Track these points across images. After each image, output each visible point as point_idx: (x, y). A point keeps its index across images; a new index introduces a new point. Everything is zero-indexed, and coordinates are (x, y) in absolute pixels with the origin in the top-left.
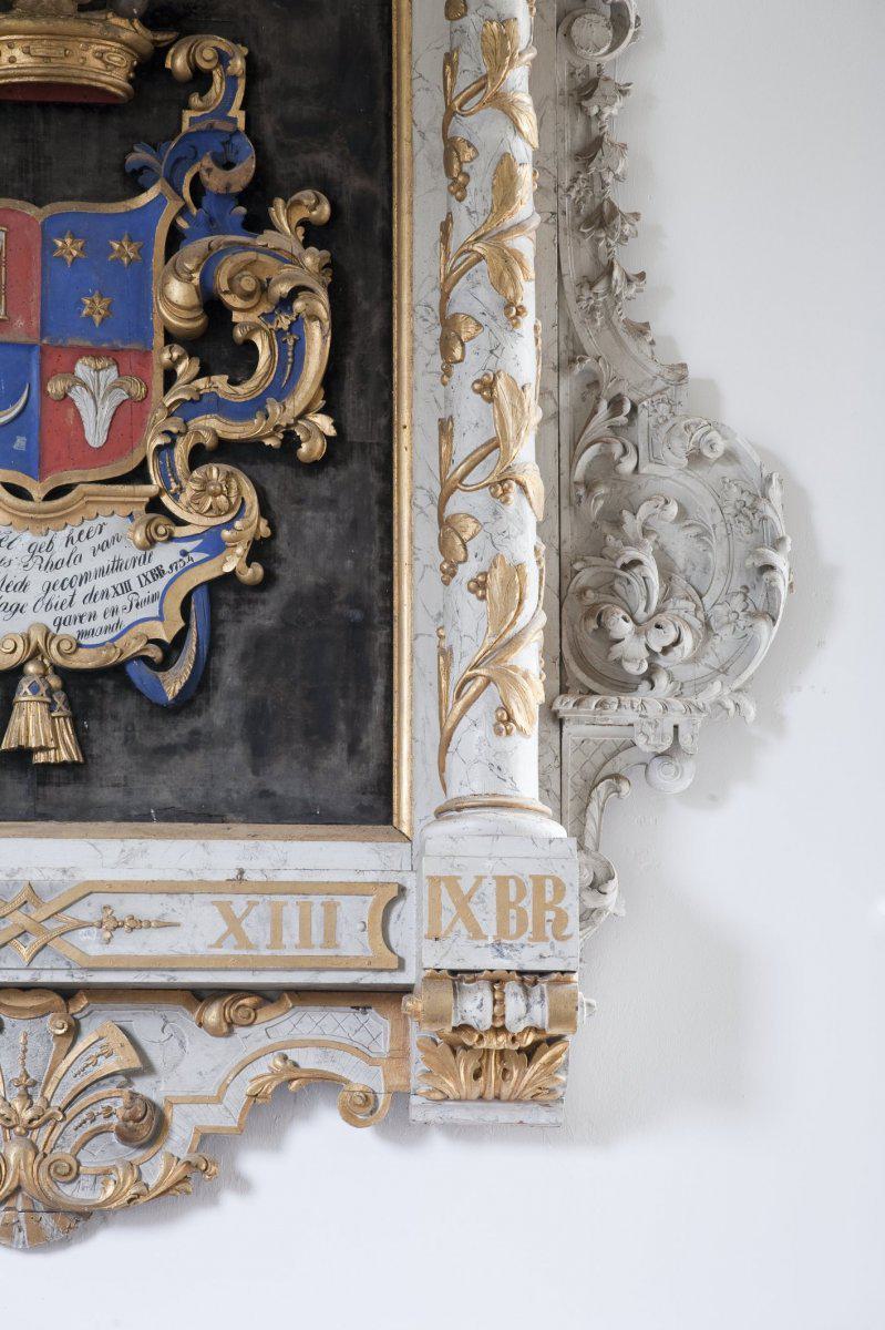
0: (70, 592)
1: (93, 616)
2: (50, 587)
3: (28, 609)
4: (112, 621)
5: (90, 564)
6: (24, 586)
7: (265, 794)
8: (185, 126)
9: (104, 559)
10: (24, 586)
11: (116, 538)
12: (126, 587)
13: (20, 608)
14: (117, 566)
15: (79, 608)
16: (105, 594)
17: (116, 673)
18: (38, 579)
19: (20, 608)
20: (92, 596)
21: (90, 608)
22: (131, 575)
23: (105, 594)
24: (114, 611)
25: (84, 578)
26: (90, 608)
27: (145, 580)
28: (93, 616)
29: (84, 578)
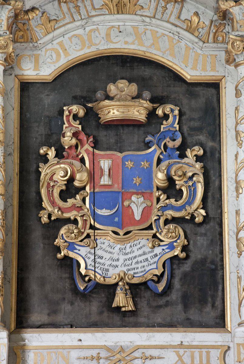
0: (131, 261)
1: (138, 268)
2: (125, 260)
4: (143, 269)
5: (137, 253)
6: (118, 260)
7: (188, 319)
8: (162, 130)
9: (141, 252)
10: (118, 260)
11: (144, 246)
13: (117, 266)
14: (144, 254)
15: (134, 266)
16: (141, 262)
18: (122, 258)
19: (117, 266)
21: (137, 266)
22: (148, 256)
23: (141, 262)
24: (144, 267)
25: (135, 257)
26: (137, 266)
27: (152, 258)
28: (138, 268)
29: (135, 257)
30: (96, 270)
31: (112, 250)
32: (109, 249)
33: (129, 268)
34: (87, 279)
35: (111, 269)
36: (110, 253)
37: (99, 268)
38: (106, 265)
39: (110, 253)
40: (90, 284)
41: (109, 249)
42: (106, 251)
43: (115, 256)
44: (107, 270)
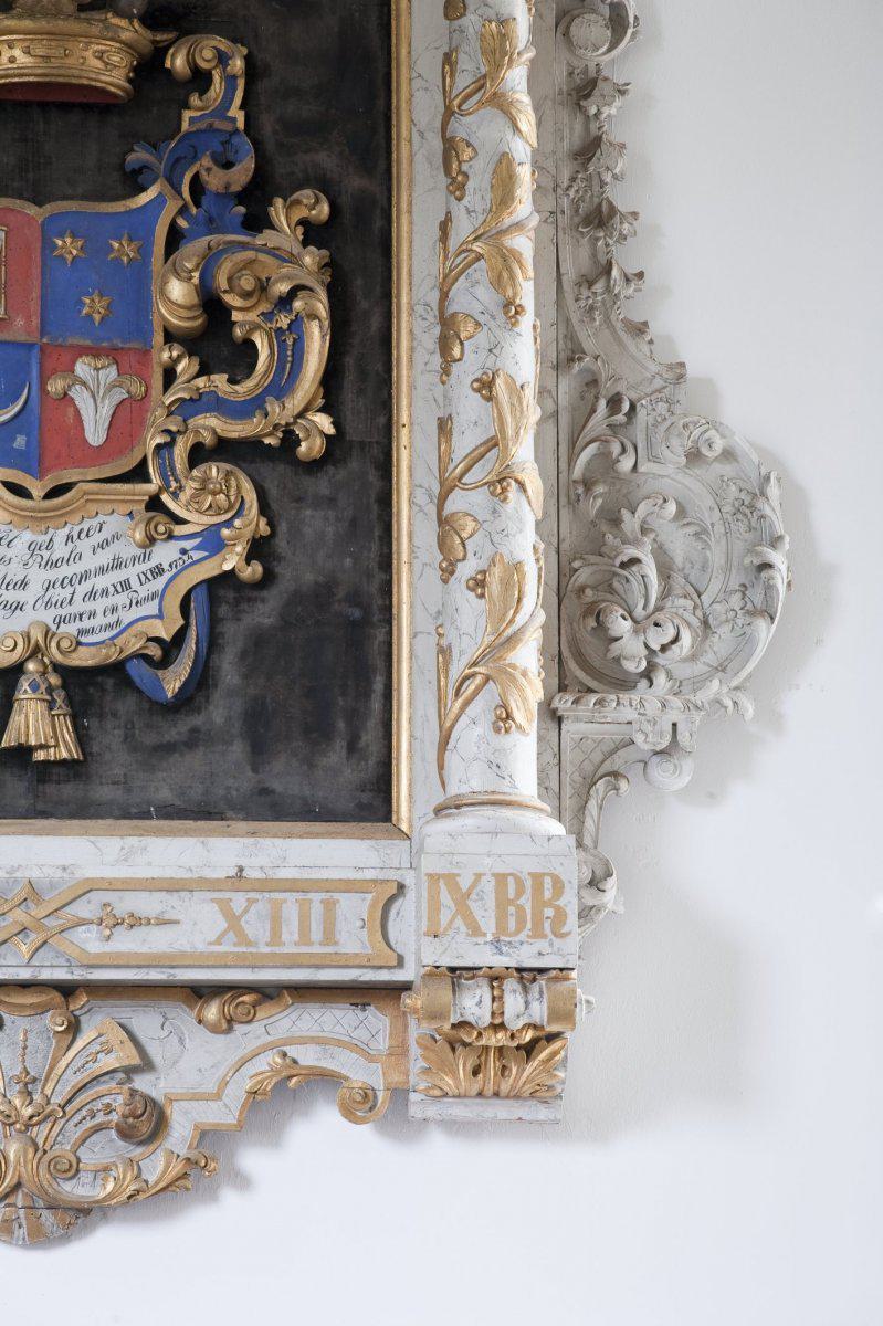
0: (69, 590)
1: (93, 615)
2: (50, 585)
3: (28, 608)
4: (111, 619)
5: (90, 562)
6: (24, 584)
7: (265, 791)
8: (185, 126)
9: (104, 558)
10: (24, 584)
11: (116, 537)
12: (126, 585)
13: (20, 607)
14: (117, 564)
15: (79, 606)
16: (105, 592)
17: (116, 671)
18: (38, 577)
19: (20, 607)
20: (92, 595)
21: (90, 606)
22: (131, 573)
23: (105, 592)
24: (114, 609)
25: (84, 576)
26: (90, 606)
27: (144, 578)
28: (93, 615)
29: (84, 576)
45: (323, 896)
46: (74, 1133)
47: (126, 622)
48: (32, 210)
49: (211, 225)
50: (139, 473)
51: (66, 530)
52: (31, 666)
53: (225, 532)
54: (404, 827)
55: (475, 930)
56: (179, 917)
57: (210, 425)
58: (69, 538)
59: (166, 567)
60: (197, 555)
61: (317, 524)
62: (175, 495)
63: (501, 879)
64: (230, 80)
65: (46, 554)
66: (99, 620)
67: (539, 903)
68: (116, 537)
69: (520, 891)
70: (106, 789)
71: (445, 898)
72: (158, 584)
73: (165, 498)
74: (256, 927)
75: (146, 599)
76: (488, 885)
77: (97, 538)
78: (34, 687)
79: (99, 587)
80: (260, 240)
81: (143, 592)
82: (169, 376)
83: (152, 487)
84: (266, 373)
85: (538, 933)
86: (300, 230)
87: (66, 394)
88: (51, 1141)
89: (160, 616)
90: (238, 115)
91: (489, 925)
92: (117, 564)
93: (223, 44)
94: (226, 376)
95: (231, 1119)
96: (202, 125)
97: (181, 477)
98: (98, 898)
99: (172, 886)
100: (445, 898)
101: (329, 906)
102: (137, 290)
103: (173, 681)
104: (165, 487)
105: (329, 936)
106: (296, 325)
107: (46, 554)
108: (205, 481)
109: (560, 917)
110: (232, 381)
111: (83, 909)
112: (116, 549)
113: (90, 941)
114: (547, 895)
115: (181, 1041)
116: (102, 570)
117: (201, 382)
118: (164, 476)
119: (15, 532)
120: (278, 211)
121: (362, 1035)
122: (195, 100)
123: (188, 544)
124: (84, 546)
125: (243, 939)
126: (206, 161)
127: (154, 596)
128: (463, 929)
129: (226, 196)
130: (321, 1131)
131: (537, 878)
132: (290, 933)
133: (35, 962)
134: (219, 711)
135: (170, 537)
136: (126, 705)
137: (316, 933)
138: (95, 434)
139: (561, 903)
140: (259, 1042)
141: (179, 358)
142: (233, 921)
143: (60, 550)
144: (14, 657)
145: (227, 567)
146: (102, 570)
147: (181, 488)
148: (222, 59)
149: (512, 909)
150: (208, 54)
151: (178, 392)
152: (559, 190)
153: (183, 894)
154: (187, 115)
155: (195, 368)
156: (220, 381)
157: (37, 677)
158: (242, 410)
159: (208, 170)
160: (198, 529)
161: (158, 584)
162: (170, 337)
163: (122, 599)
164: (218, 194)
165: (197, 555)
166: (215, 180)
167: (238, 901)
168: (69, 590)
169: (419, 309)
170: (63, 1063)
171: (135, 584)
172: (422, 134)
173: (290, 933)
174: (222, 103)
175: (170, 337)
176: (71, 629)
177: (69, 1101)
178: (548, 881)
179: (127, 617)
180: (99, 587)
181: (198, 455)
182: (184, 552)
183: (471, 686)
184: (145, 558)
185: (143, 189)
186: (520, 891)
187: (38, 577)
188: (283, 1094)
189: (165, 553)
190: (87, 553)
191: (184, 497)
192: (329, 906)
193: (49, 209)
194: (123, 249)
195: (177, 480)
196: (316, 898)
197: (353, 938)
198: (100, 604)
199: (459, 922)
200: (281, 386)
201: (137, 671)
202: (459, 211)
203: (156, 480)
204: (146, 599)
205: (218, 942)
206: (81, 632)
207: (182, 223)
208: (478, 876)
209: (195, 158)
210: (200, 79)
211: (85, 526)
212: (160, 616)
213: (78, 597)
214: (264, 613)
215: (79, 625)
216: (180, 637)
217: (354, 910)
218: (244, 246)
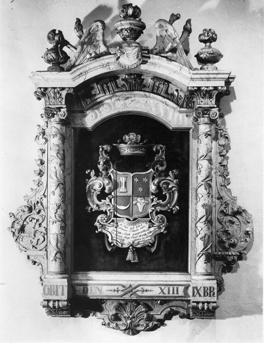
0: (137, 235)
1: (140, 239)
2: (134, 234)
3: (130, 238)
4: (143, 240)
5: (140, 231)
6: (129, 234)
7: (168, 267)
8: (155, 159)
9: (142, 230)
10: (129, 234)
11: (144, 227)
12: (146, 234)
13: (129, 238)
14: (144, 231)
15: (138, 238)
16: (142, 236)
17: (144, 248)
18: (132, 233)
19: (129, 238)
20: (140, 236)
21: (140, 238)
22: (146, 232)
23: (142, 236)
24: (144, 238)
25: (139, 233)
26: (140, 238)
27: (148, 233)
28: (140, 239)
29: (139, 233)
30: (118, 240)
31: (126, 229)
32: (124, 228)
33: (136, 239)
34: (112, 245)
35: (125, 239)
36: (125, 230)
37: (119, 239)
38: (123, 237)
39: (125, 230)
40: (114, 248)
41: (124, 228)
42: (123, 230)
43: (128, 233)
44: (124, 240)
45: (176, 287)
46: (138, 320)
47: (146, 240)
48: (130, 174)
49: (160, 176)
50: (147, 216)
51: (136, 226)
52: (131, 247)
53: (161, 226)
54: (189, 272)
55: (200, 296)
56: (154, 290)
57: (158, 209)
58: (137, 227)
59: (152, 231)
60: (157, 229)
61: (176, 224)
62: (153, 220)
63: (204, 288)
64: (162, 152)
65: (133, 230)
66: (141, 240)
67: (210, 292)
68: (144, 227)
69: (207, 289)
70: (143, 266)
71: (195, 291)
72: (151, 234)
73: (152, 220)
74: (166, 291)
75: (149, 236)
76: (202, 288)
77: (141, 227)
78: (131, 251)
79: (141, 235)
80: (167, 178)
81: (148, 235)
82: (152, 200)
83: (150, 219)
84: (168, 200)
85: (210, 296)
86: (174, 176)
87: (136, 204)
88: (135, 321)
89: (151, 239)
90: (164, 157)
91: (202, 294)
92: (144, 231)
93: (162, 146)
94: (162, 200)
95: (162, 318)
96: (158, 160)
97: (154, 217)
98: (141, 287)
99: (152, 285)
100: (195, 291)
101: (177, 288)
102: (147, 187)
103: (153, 250)
104: (152, 218)
105: (177, 293)
106: (173, 192)
107: (133, 230)
108: (158, 218)
109: (214, 294)
110: (162, 201)
111: (138, 289)
112: (144, 229)
113: (139, 293)
114: (212, 290)
115: (155, 306)
116: (142, 232)
117: (158, 201)
118: (151, 217)
119: (128, 226)
120: (170, 173)
121: (183, 305)
122: (157, 155)
123: (156, 228)
124: (139, 228)
125: (164, 293)
126: (159, 166)
127: (150, 236)
128: (198, 296)
129: (162, 171)
130: (176, 319)
131: (210, 287)
132: (171, 292)
133: (131, 297)
134: (160, 254)
135: (153, 226)
136: (145, 253)
137: (175, 292)
138: (140, 210)
139: (214, 291)
140: (167, 307)
141: (154, 198)
142: (162, 291)
143: (135, 229)
144: (128, 246)
145: (162, 231)
146: (142, 232)
147: (154, 219)
148: (161, 148)
149: (206, 292)
150: (159, 148)
151: (154, 203)
152: (217, 169)
153: (154, 286)
154: (156, 157)
155: (157, 199)
156: (161, 201)
157: (131, 249)
158: (164, 206)
159: (159, 167)
160: (157, 225)
161: (151, 234)
162: (153, 194)
163: (145, 236)
164: (160, 171)
165: (157, 229)
166: (160, 169)
167: (163, 287)
168: (137, 235)
169: (193, 189)
170: (136, 309)
171: (147, 234)
172: (194, 160)
173: (171, 292)
174: (161, 156)
175: (153, 194)
176: (136, 242)
177: (137, 315)
178: (212, 288)
179: (146, 239)
180: (141, 235)
181: (157, 213)
182: (155, 229)
183: (200, 255)
184: (149, 230)
185: (148, 170)
186: (207, 289)
187: (132, 233)
188: (169, 317)
189: (152, 229)
190: (139, 229)
191: (155, 220)
192: (177, 288)
193: (134, 174)
194: (145, 180)
195: (154, 217)
196: (175, 287)
197: (181, 293)
198: (141, 237)
199: (198, 294)
200: (170, 202)
201: (147, 248)
202: (199, 176)
203: (150, 217)
204: (149, 236)
205: (160, 294)
206: (139, 242)
207: (155, 175)
208: (201, 287)
209: (157, 164)
210: (158, 152)
211: (139, 225)
212: (151, 239)
213: (138, 237)
214: (168, 238)
215: (138, 241)
216: (154, 242)
217: (181, 289)
218: (165, 180)
